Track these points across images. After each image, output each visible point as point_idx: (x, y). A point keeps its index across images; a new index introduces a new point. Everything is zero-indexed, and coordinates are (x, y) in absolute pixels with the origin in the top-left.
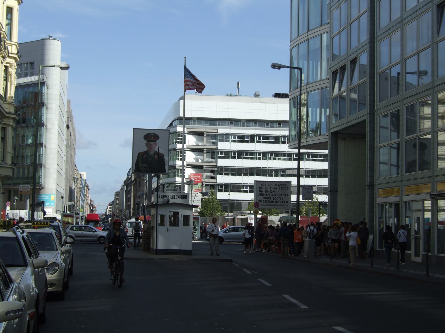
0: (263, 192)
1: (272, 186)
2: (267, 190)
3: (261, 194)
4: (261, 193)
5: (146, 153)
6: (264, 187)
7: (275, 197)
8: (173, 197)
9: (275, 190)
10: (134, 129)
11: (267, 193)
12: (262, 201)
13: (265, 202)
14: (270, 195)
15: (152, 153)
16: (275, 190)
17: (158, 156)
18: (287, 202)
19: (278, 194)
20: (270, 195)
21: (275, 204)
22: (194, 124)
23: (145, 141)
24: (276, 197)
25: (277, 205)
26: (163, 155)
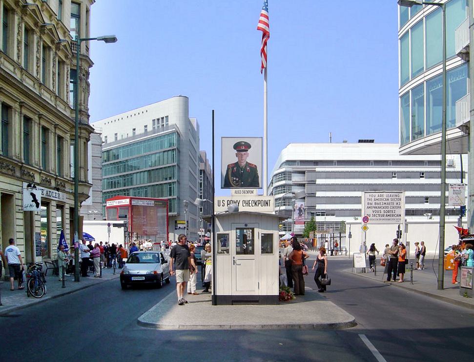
0: (372, 204)
2: (377, 202)
4: (370, 206)
5: (237, 164)
6: (373, 198)
8: (247, 203)
9: (386, 202)
10: (222, 138)
11: (377, 205)
12: (371, 215)
15: (243, 164)
16: (386, 202)
17: (250, 167)
19: (389, 206)
21: (387, 218)
22: (298, 165)
23: (235, 151)
26: (255, 166)
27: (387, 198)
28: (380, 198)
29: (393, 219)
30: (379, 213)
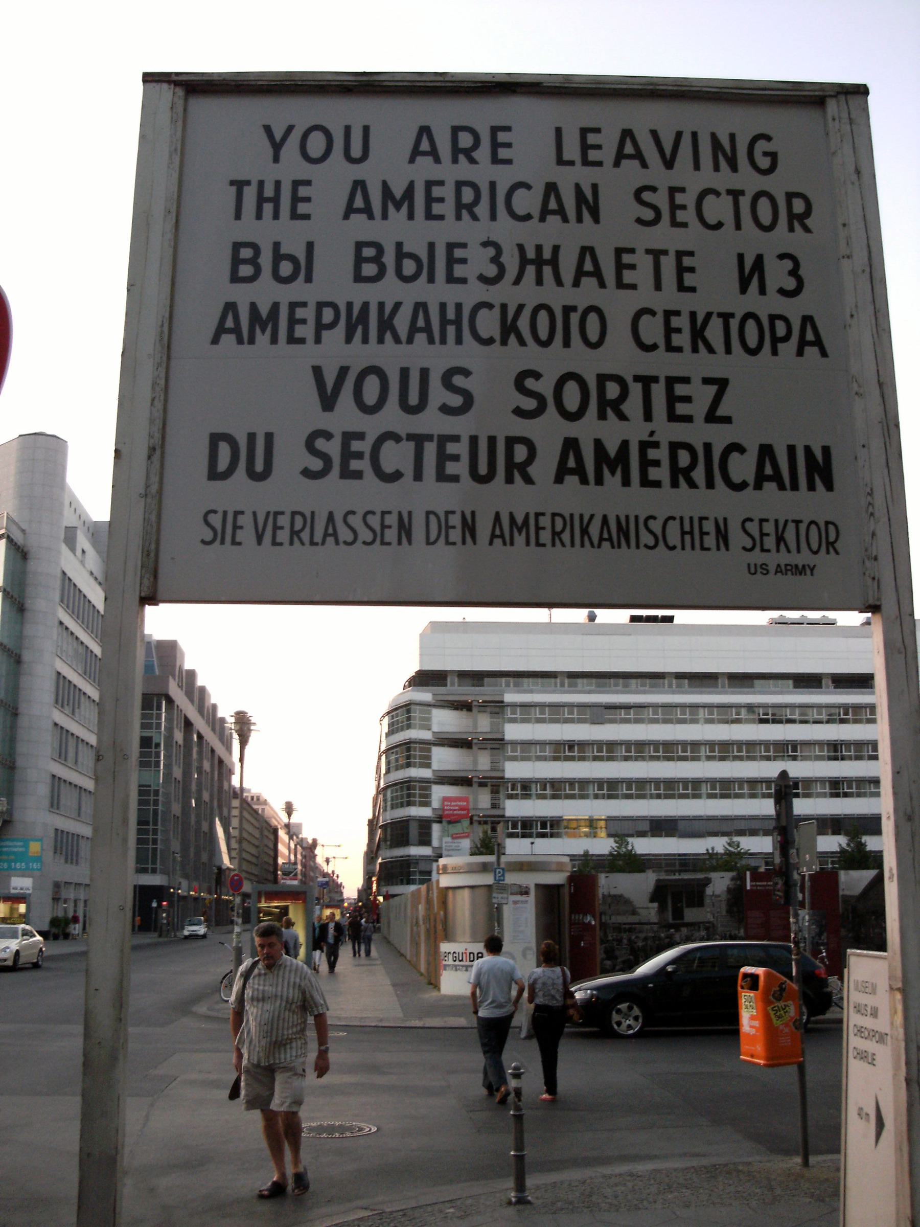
0: (304, 267)
1: (482, 171)
3: (263, 321)
4: (265, 292)
6: (331, 181)
7: (552, 362)
9: (567, 236)
11: (389, 290)
12: (291, 457)
13: (340, 459)
14: (454, 323)
16: (567, 236)
18: (821, 469)
19: (619, 307)
20: (454, 323)
21: (573, 498)
24: (589, 364)
25: (621, 533)
27: (568, 180)
28: (450, 172)
29: (693, 533)
30: (431, 422)
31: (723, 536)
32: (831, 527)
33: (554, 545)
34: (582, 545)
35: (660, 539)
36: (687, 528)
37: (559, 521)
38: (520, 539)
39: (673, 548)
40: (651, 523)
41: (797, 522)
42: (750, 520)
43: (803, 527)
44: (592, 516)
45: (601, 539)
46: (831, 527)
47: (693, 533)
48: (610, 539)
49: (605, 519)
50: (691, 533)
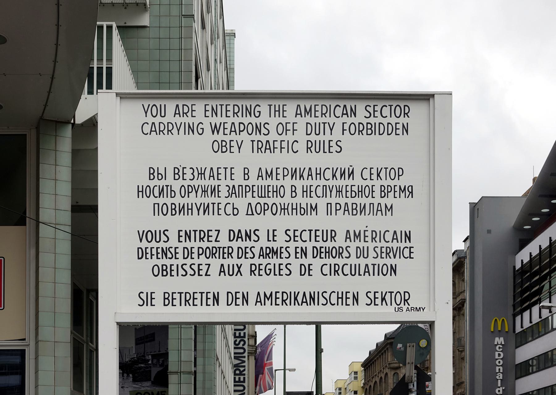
25: (312, 299)
29: (342, 298)
31: (356, 299)
32: (407, 294)
33: (282, 305)
34: (295, 305)
35: (328, 301)
36: (340, 296)
37: (285, 294)
38: (268, 302)
39: (334, 304)
40: (324, 294)
41: (391, 293)
42: (370, 292)
43: (393, 295)
44: (299, 292)
45: (302, 302)
46: (407, 294)
47: (342, 298)
48: (306, 302)
49: (304, 294)
50: (342, 298)
